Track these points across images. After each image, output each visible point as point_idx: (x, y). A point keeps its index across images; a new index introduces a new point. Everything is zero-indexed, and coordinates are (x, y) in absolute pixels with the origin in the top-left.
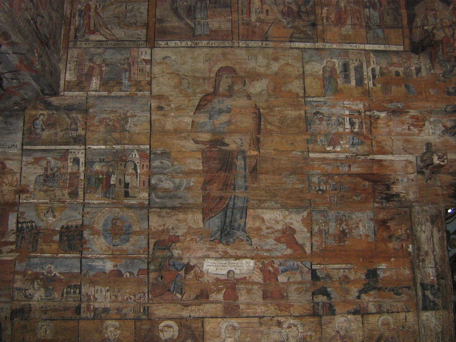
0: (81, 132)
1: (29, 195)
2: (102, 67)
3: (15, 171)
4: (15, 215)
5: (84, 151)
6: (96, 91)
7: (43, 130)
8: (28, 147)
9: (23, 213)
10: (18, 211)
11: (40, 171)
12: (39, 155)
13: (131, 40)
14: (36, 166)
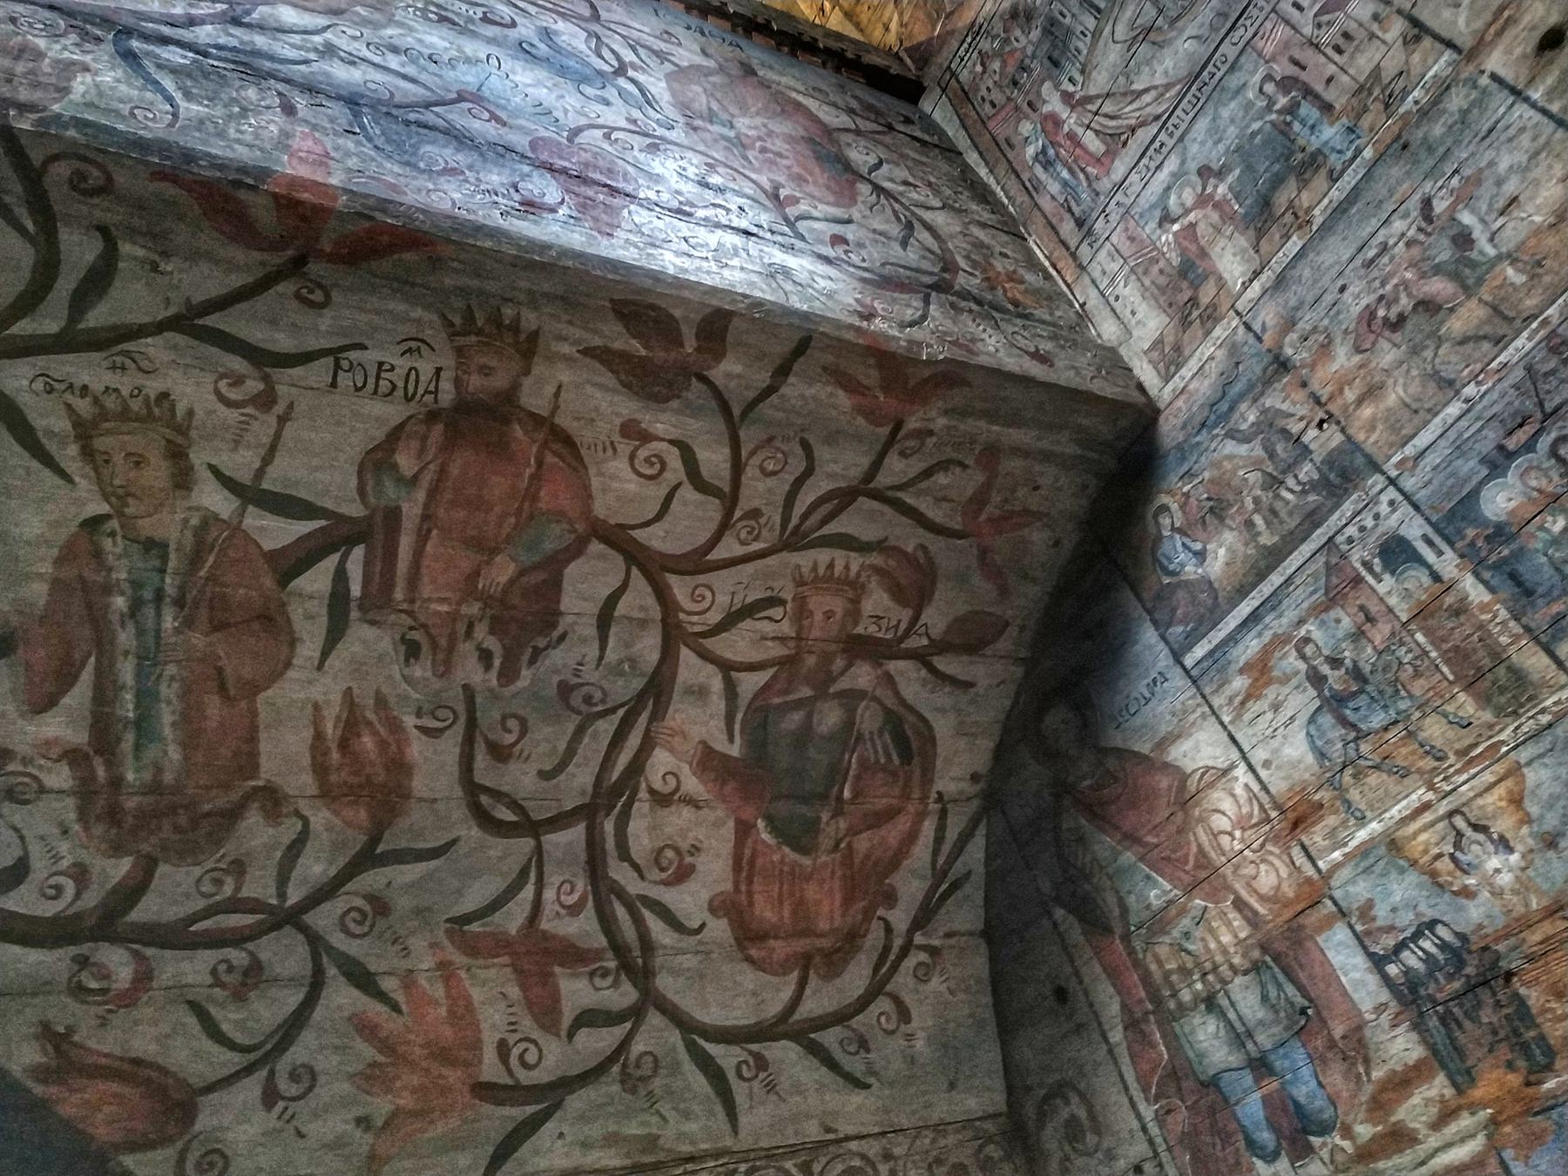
0: (1323, 442)
1: (1331, 820)
2: (1211, 196)
3: (1221, 763)
4: (1340, 933)
5: (1391, 493)
6: (1256, 274)
7: (1201, 556)
8: (1199, 651)
9: (1366, 911)
10: (1343, 913)
11: (1302, 701)
12: (1251, 646)
13: (1228, 25)
14: (1271, 693)
